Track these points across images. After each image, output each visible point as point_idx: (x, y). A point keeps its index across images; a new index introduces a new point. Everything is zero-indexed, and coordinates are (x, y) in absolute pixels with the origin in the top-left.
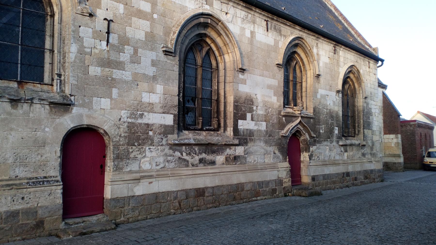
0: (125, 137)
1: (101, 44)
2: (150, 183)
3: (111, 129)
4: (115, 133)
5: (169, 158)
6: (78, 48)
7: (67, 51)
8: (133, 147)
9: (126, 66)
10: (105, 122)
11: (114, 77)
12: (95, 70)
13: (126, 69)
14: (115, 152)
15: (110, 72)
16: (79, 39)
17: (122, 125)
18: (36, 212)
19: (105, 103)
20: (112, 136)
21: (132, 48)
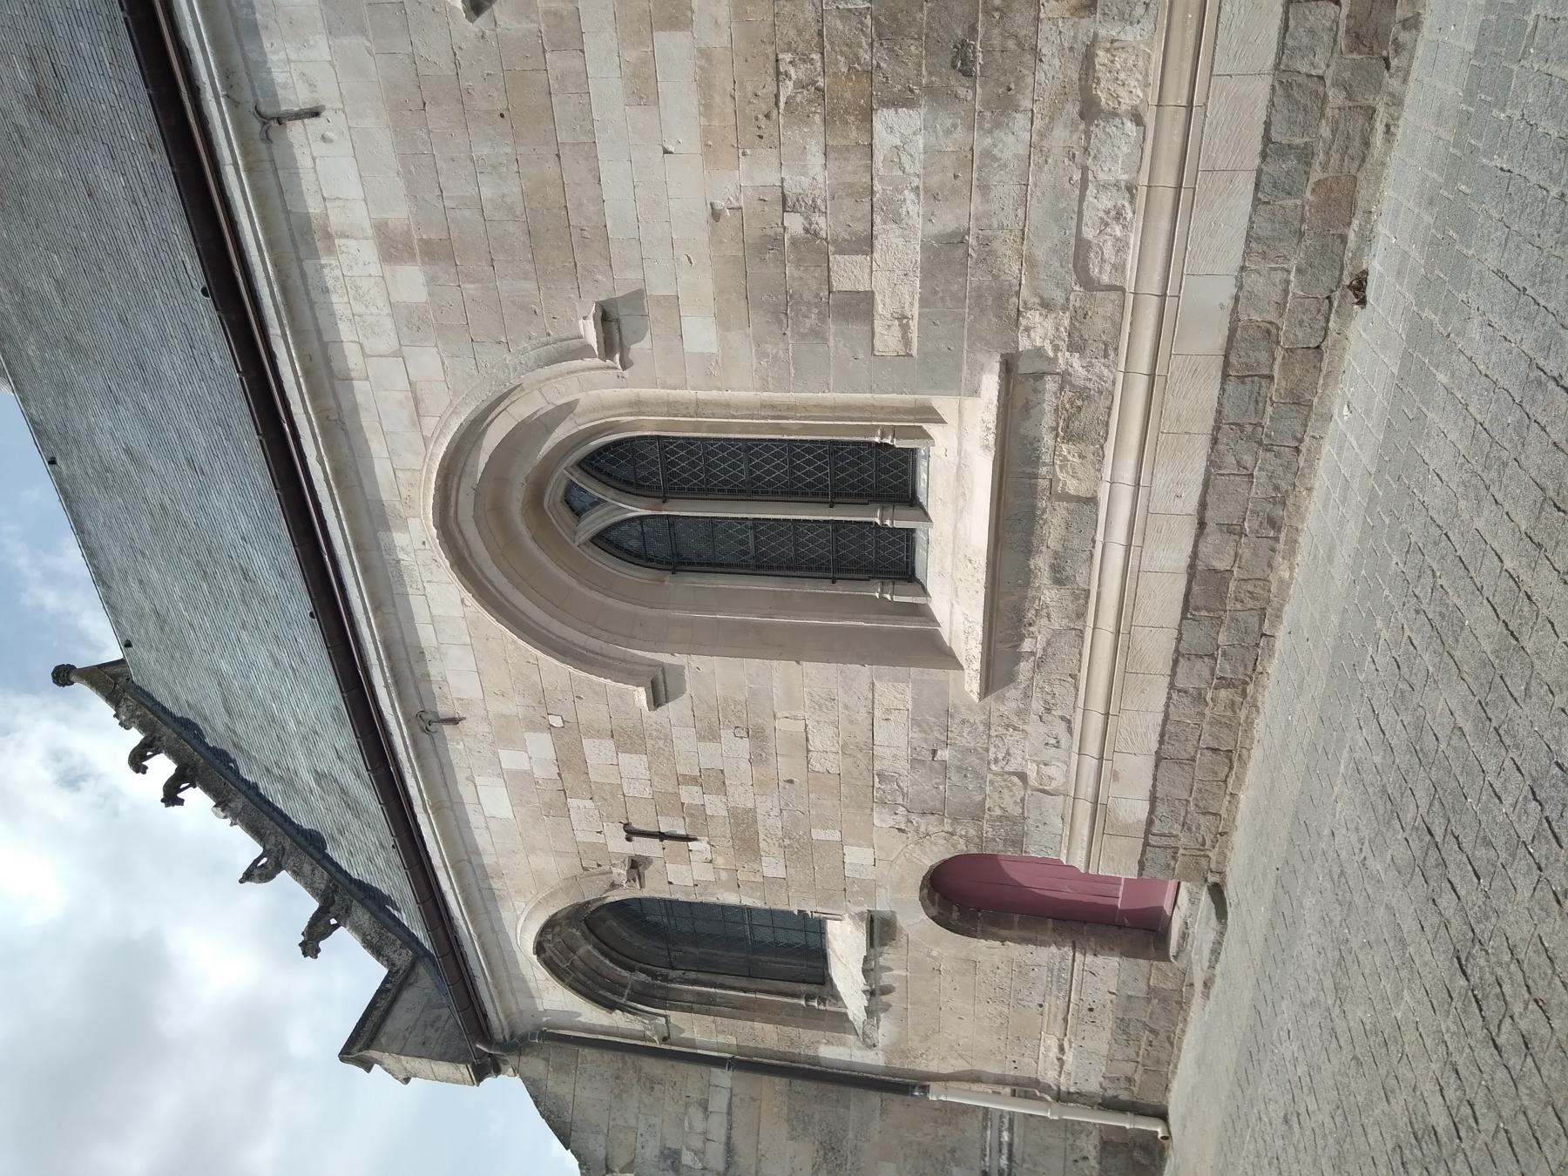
2: (1115, 776)
5: (1037, 705)
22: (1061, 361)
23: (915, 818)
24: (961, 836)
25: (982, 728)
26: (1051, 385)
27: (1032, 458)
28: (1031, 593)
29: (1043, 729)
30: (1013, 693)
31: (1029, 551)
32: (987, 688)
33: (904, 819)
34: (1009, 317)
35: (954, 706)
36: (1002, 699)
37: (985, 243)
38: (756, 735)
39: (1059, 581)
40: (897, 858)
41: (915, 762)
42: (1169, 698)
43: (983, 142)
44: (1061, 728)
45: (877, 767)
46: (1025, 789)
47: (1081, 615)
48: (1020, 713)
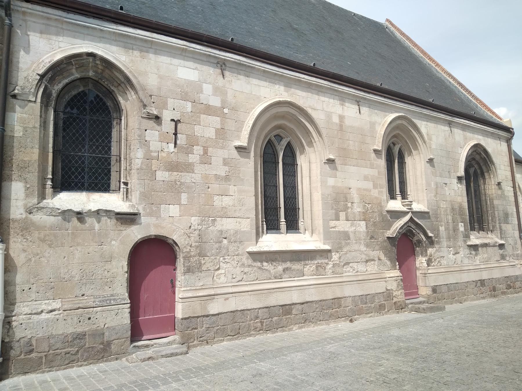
0: (197, 247)
1: (168, 147)
2: (226, 299)
3: (181, 239)
4: (185, 243)
6: (144, 153)
7: (133, 157)
8: (205, 258)
9: (195, 168)
11: (182, 181)
12: (163, 175)
13: (196, 171)
14: (186, 265)
15: (178, 176)
17: (193, 234)
18: (103, 334)
19: (174, 210)
20: (182, 247)
21: (202, 148)
22: (330, 262)
25: (237, 253)
26: (326, 261)
27: (312, 259)
28: (280, 263)
29: (239, 273)
30: (250, 262)
31: (291, 261)
32: (250, 253)
33: (196, 228)
34: (337, 250)
35: (244, 244)
36: (247, 258)
37: (349, 244)
38: (227, 178)
39: (284, 270)
40: (176, 226)
41: (221, 231)
42: (256, 309)
43: (362, 242)
44: (239, 278)
45: (218, 219)
46: (214, 270)
47: (276, 278)
48: (243, 265)
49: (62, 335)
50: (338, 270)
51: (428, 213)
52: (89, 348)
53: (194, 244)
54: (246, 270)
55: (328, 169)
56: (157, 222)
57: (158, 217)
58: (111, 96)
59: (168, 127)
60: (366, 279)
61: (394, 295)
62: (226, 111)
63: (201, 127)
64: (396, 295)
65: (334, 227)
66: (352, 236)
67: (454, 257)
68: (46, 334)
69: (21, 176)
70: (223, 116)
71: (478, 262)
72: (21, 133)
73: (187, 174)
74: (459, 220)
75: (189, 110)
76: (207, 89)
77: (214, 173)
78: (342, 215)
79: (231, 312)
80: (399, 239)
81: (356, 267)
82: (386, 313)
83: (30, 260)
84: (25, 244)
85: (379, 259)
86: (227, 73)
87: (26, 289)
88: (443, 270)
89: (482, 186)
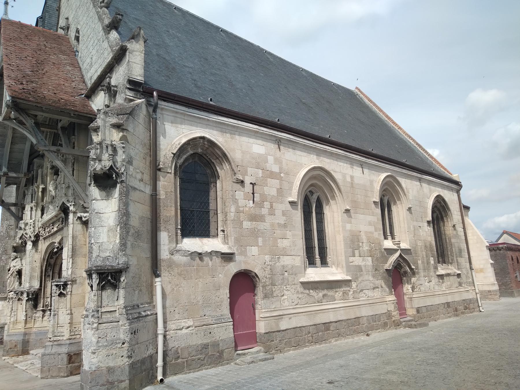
0: (270, 278)
2: (290, 318)
10: (256, 266)
11: (259, 228)
13: (266, 221)
14: (264, 292)
15: (256, 225)
16: (236, 201)
17: (267, 268)
19: (254, 250)
23: (269, 267)
24: (266, 280)
25: (293, 283)
26: (349, 289)
27: (340, 287)
28: (321, 290)
29: (296, 298)
31: (327, 289)
32: (302, 283)
33: (268, 264)
35: (297, 276)
36: (300, 287)
38: (285, 226)
39: (324, 296)
41: (283, 266)
42: (308, 326)
44: (296, 303)
45: (281, 257)
46: (280, 296)
47: (318, 302)
48: (298, 292)
49: (195, 345)
50: (356, 295)
51: (410, 250)
52: (211, 355)
53: (268, 276)
54: (300, 296)
55: (346, 217)
56: (245, 259)
57: (246, 256)
58: (210, 166)
59: (248, 188)
60: (375, 302)
61: (393, 314)
62: (282, 175)
63: (268, 187)
64: (394, 315)
65: (352, 262)
66: (363, 269)
67: (429, 284)
68: (186, 345)
69: (165, 227)
70: (281, 179)
71: (444, 289)
72: (164, 196)
73: (261, 223)
74: (430, 255)
75: (260, 175)
76: (271, 159)
77: (277, 221)
78: (357, 252)
79: (294, 328)
80: (393, 270)
81: (367, 293)
82: (388, 329)
83: (173, 289)
84: (170, 277)
85: (382, 287)
86: (282, 147)
87: (172, 311)
88: (422, 295)
89: (442, 228)
